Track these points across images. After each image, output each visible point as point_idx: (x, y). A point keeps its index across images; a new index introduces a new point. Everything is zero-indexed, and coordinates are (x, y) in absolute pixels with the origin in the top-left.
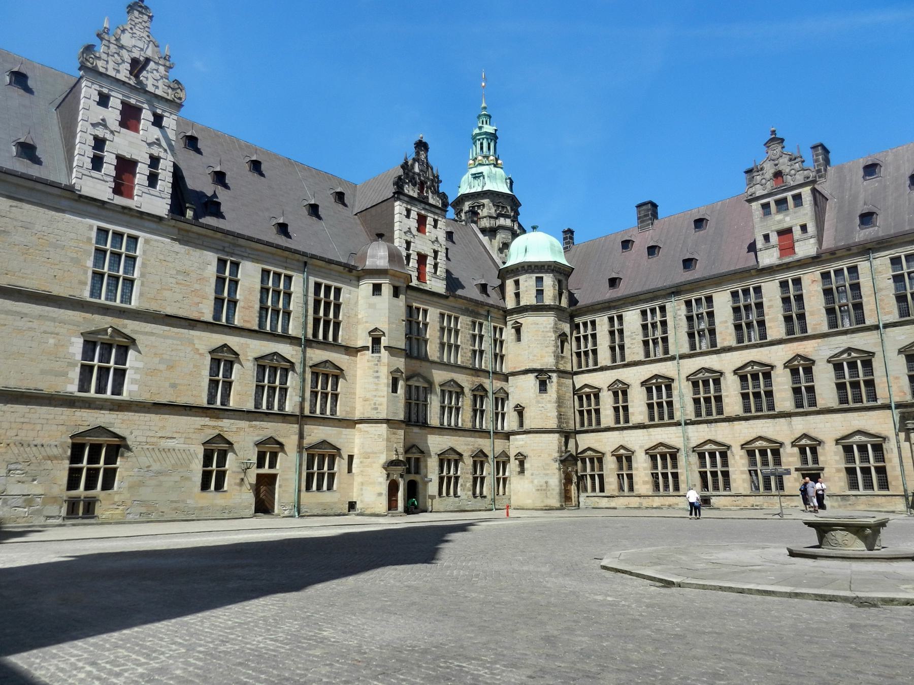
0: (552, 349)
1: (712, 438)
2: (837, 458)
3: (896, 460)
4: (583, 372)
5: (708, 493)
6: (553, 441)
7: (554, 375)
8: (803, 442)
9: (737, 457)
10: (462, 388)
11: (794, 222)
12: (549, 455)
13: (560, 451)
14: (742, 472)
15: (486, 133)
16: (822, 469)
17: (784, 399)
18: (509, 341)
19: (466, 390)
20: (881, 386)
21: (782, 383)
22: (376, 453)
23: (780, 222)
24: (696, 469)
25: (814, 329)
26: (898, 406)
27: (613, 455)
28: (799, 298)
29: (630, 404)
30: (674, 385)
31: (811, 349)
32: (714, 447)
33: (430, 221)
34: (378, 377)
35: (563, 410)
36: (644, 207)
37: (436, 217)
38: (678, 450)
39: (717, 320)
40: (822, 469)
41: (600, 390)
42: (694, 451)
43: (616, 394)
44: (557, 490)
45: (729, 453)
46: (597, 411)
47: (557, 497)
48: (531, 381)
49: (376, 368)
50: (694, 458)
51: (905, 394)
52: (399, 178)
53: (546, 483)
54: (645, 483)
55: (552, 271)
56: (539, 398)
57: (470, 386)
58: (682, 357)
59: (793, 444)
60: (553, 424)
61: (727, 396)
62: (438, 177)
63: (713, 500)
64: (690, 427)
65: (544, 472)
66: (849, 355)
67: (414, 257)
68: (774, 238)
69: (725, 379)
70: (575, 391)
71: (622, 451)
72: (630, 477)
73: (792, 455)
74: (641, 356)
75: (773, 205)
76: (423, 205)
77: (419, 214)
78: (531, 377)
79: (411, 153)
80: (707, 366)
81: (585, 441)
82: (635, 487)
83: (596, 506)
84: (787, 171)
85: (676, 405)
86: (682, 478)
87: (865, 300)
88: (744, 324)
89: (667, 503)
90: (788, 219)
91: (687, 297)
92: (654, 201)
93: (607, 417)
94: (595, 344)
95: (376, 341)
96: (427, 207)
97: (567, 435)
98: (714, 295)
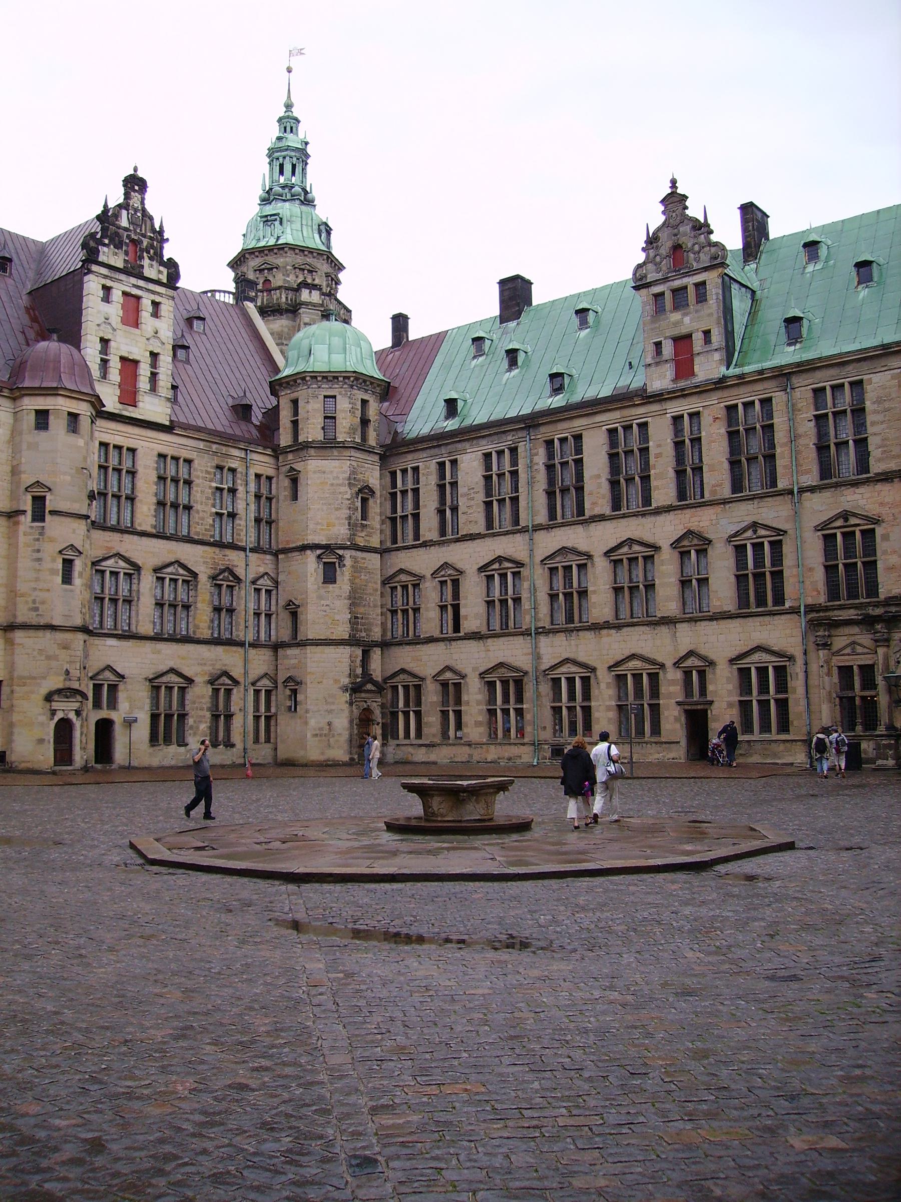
2: (730, 687)
3: (801, 691)
4: (398, 549)
5: (562, 740)
8: (689, 662)
9: (603, 686)
10: (195, 575)
11: (695, 325)
12: (336, 681)
14: (608, 708)
16: (711, 703)
17: (667, 598)
18: (281, 498)
19: (203, 578)
20: (791, 580)
21: (667, 571)
22: (35, 678)
23: (677, 324)
24: (547, 703)
25: (714, 492)
26: (810, 609)
28: (697, 441)
30: (525, 572)
31: (707, 523)
32: (574, 669)
33: (146, 303)
34: (39, 560)
35: (362, 610)
37: (158, 299)
40: (711, 703)
41: (421, 578)
44: (346, 735)
47: (346, 746)
48: (311, 564)
49: (37, 545)
50: (545, 688)
51: (819, 593)
52: (92, 235)
53: (329, 724)
54: (478, 724)
56: (322, 591)
57: (211, 572)
58: (538, 528)
59: (676, 664)
60: (342, 631)
62: (161, 232)
65: (326, 707)
66: (755, 532)
67: (115, 365)
68: (668, 349)
69: (593, 564)
71: (448, 675)
72: (458, 714)
73: (673, 682)
74: (480, 527)
75: (668, 296)
76: (133, 280)
77: (125, 294)
78: (311, 557)
79: (116, 197)
80: (569, 544)
84: (690, 245)
87: (778, 450)
89: (506, 755)
90: (687, 320)
92: (527, 277)
93: (430, 620)
94: (417, 505)
95: (39, 502)
96: (141, 283)
98: (584, 433)
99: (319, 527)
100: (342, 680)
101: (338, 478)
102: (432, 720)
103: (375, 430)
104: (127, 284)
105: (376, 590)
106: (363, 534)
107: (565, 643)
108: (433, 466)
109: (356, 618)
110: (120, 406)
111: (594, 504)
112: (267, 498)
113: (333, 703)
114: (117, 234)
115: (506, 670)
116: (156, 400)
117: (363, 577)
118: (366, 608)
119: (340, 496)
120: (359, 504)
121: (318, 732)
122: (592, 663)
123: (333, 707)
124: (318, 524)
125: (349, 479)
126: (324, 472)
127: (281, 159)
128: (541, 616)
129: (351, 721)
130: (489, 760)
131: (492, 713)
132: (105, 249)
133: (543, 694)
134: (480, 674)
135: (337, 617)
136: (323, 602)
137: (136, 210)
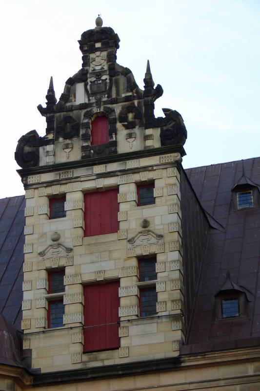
37: (144, 177)
62: (148, 80)
76: (99, 169)
96: (113, 167)
104: (91, 179)
110: (85, 358)
114: (68, 119)
116: (151, 327)
132: (50, 148)
137: (98, 75)
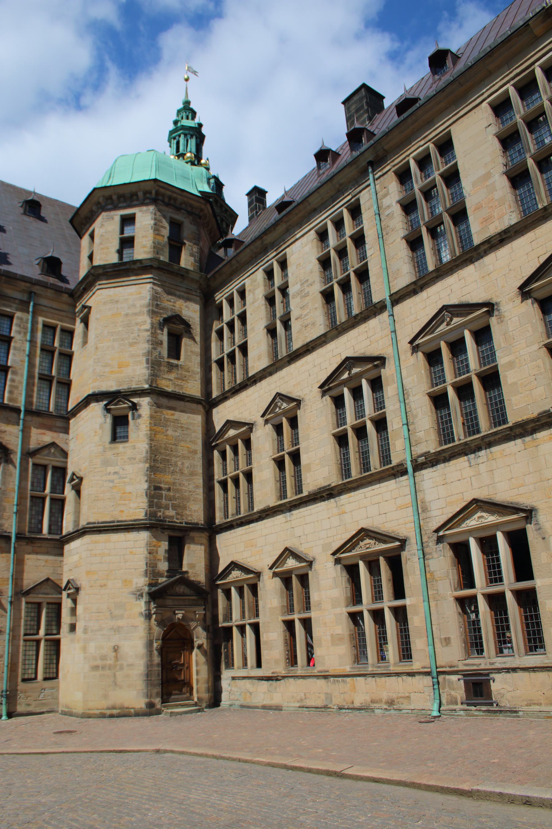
0: (145, 347)
1: (482, 495)
6: (136, 547)
7: (145, 404)
12: (126, 582)
13: (152, 571)
15: (183, 127)
27: (275, 575)
29: (302, 446)
32: (491, 519)
35: (168, 478)
36: (356, 98)
38: (403, 542)
39: (467, 182)
41: (250, 426)
42: (440, 540)
43: (279, 429)
45: (530, 529)
46: (249, 476)
50: (442, 561)
53: (116, 649)
55: (154, 201)
56: (109, 454)
60: (137, 509)
61: (511, 365)
63: (499, 685)
64: (427, 473)
69: (501, 318)
70: (211, 440)
71: (291, 563)
72: (307, 623)
80: (454, 301)
81: (232, 546)
82: (318, 652)
83: (248, 702)
85: (394, 423)
86: (415, 621)
88: (531, 163)
89: (385, 696)
91: (397, 161)
97: (177, 538)
99: (107, 369)
100: (135, 581)
101: (134, 306)
102: (273, 637)
103: (192, 255)
105: (195, 452)
106: (172, 376)
107: (468, 472)
108: (260, 275)
109: (160, 488)
111: (487, 220)
112: (61, 354)
113: (121, 617)
115: (372, 542)
117: (170, 432)
118: (178, 476)
119: (136, 328)
120: (164, 337)
121: (99, 662)
122: (525, 501)
123: (120, 623)
124: (107, 365)
125: (149, 305)
126: (117, 302)
127: (177, 138)
128: (421, 434)
129: (150, 644)
130: (357, 704)
131: (355, 618)
133: (437, 574)
134: (334, 554)
135: (129, 489)
136: (110, 469)
